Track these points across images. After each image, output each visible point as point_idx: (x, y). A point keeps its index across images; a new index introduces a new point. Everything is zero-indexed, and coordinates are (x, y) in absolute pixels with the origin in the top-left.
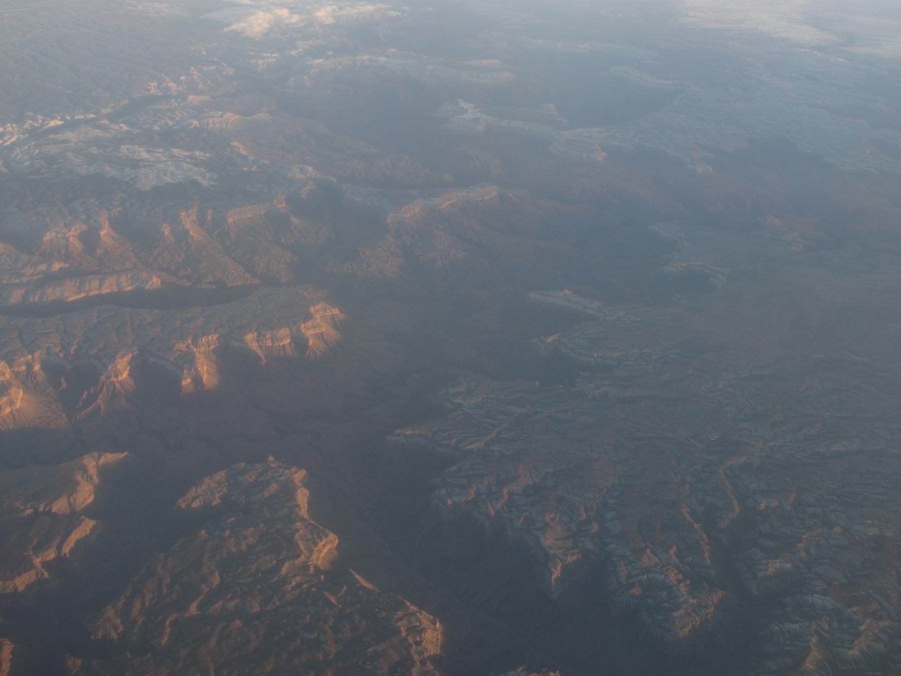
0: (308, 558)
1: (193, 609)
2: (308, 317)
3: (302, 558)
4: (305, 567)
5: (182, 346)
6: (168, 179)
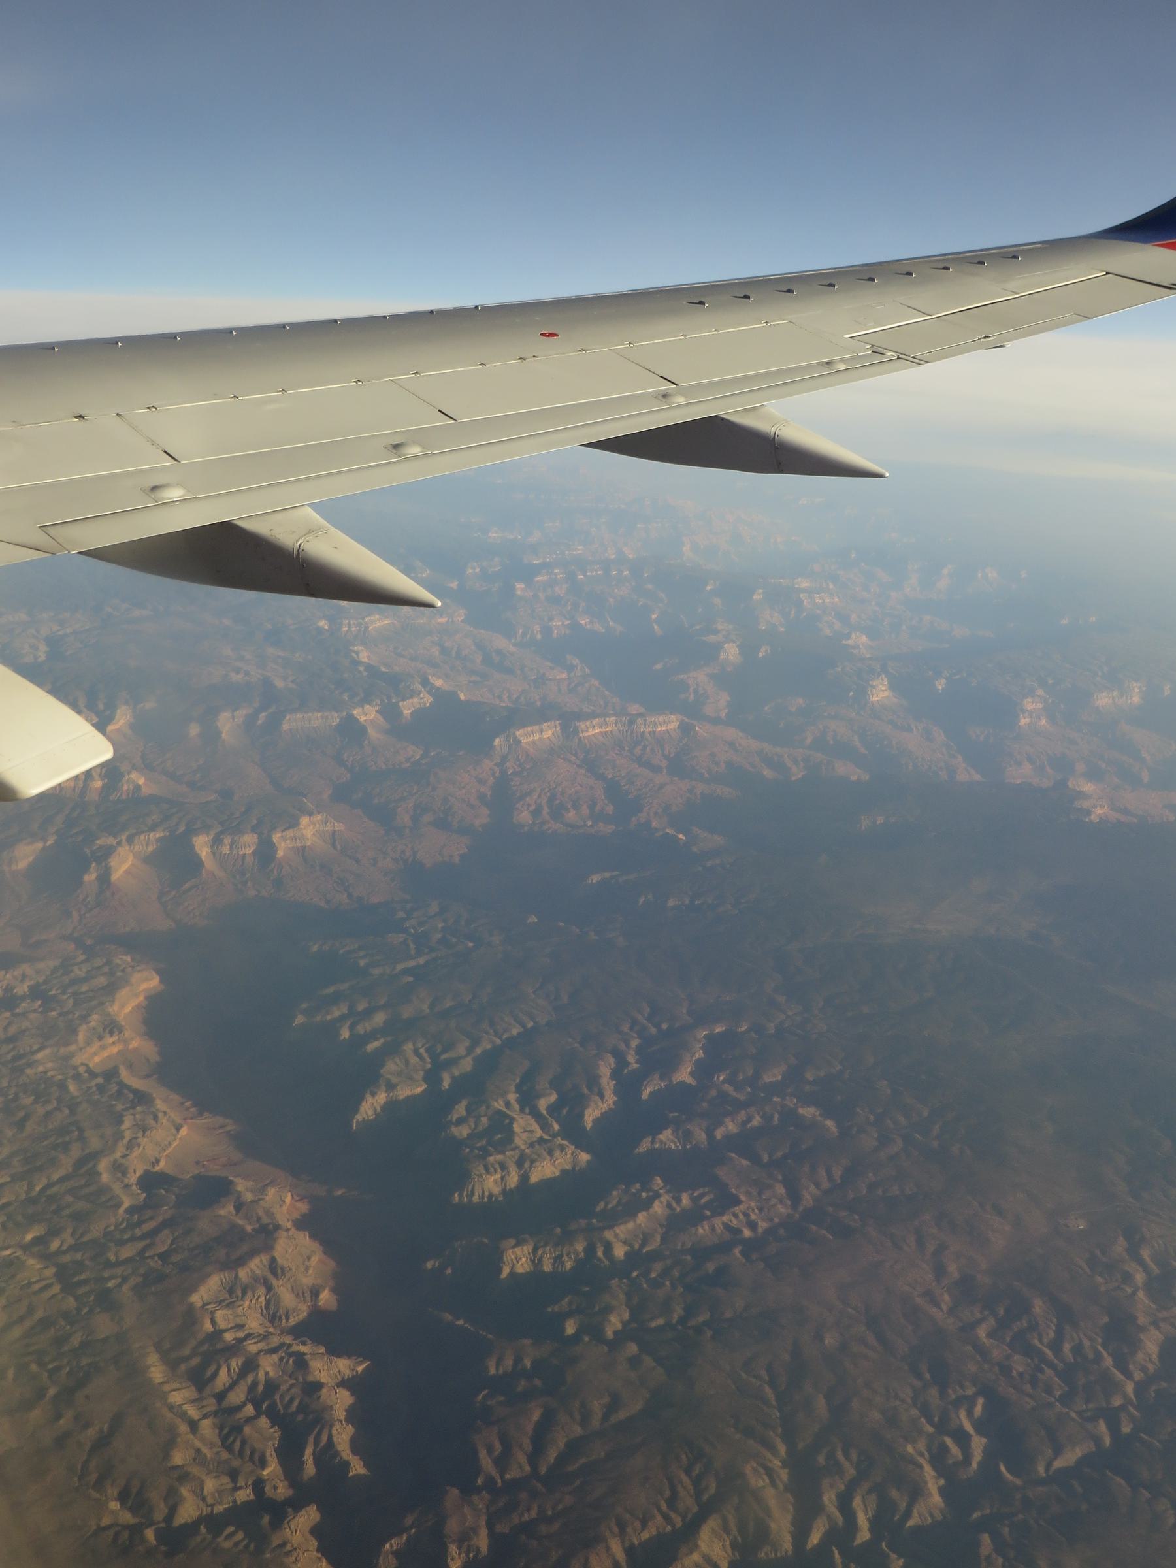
3: (73, 1048)
6: (236, 678)
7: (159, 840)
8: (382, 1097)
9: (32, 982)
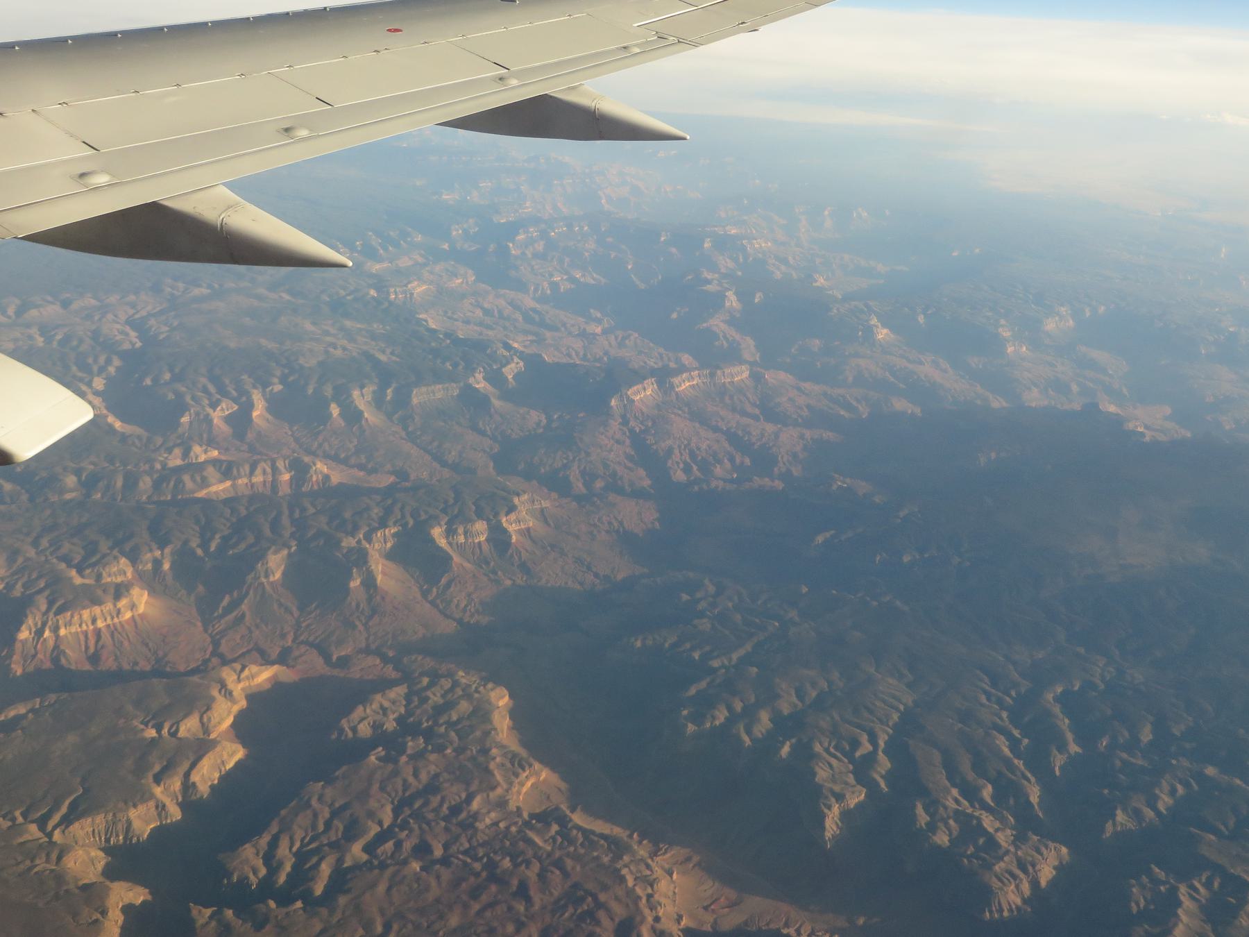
0: (507, 791)
1: (356, 851)
2: (512, 509)
3: (499, 791)
4: (502, 804)
5: (349, 542)
6: (338, 353)
7: (394, 535)
8: (836, 809)
9: (396, 715)
